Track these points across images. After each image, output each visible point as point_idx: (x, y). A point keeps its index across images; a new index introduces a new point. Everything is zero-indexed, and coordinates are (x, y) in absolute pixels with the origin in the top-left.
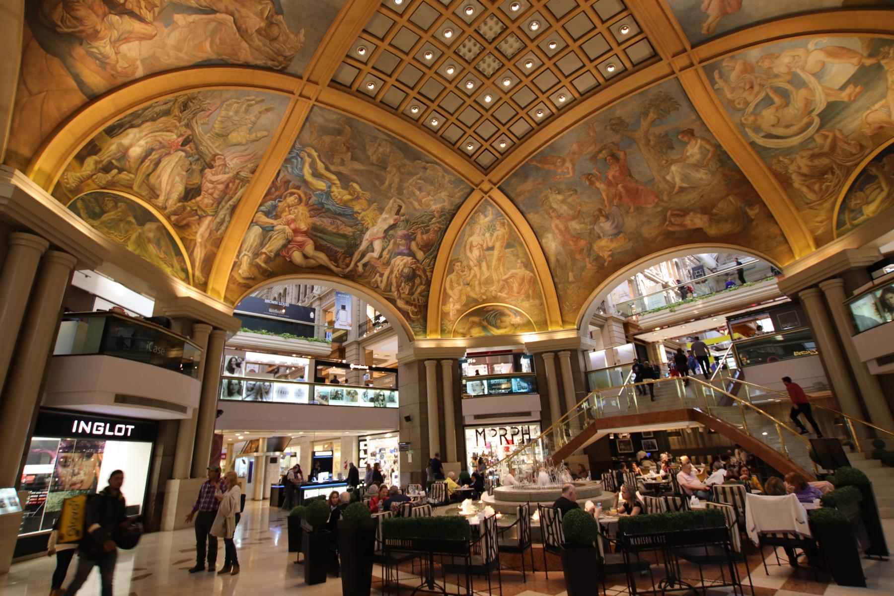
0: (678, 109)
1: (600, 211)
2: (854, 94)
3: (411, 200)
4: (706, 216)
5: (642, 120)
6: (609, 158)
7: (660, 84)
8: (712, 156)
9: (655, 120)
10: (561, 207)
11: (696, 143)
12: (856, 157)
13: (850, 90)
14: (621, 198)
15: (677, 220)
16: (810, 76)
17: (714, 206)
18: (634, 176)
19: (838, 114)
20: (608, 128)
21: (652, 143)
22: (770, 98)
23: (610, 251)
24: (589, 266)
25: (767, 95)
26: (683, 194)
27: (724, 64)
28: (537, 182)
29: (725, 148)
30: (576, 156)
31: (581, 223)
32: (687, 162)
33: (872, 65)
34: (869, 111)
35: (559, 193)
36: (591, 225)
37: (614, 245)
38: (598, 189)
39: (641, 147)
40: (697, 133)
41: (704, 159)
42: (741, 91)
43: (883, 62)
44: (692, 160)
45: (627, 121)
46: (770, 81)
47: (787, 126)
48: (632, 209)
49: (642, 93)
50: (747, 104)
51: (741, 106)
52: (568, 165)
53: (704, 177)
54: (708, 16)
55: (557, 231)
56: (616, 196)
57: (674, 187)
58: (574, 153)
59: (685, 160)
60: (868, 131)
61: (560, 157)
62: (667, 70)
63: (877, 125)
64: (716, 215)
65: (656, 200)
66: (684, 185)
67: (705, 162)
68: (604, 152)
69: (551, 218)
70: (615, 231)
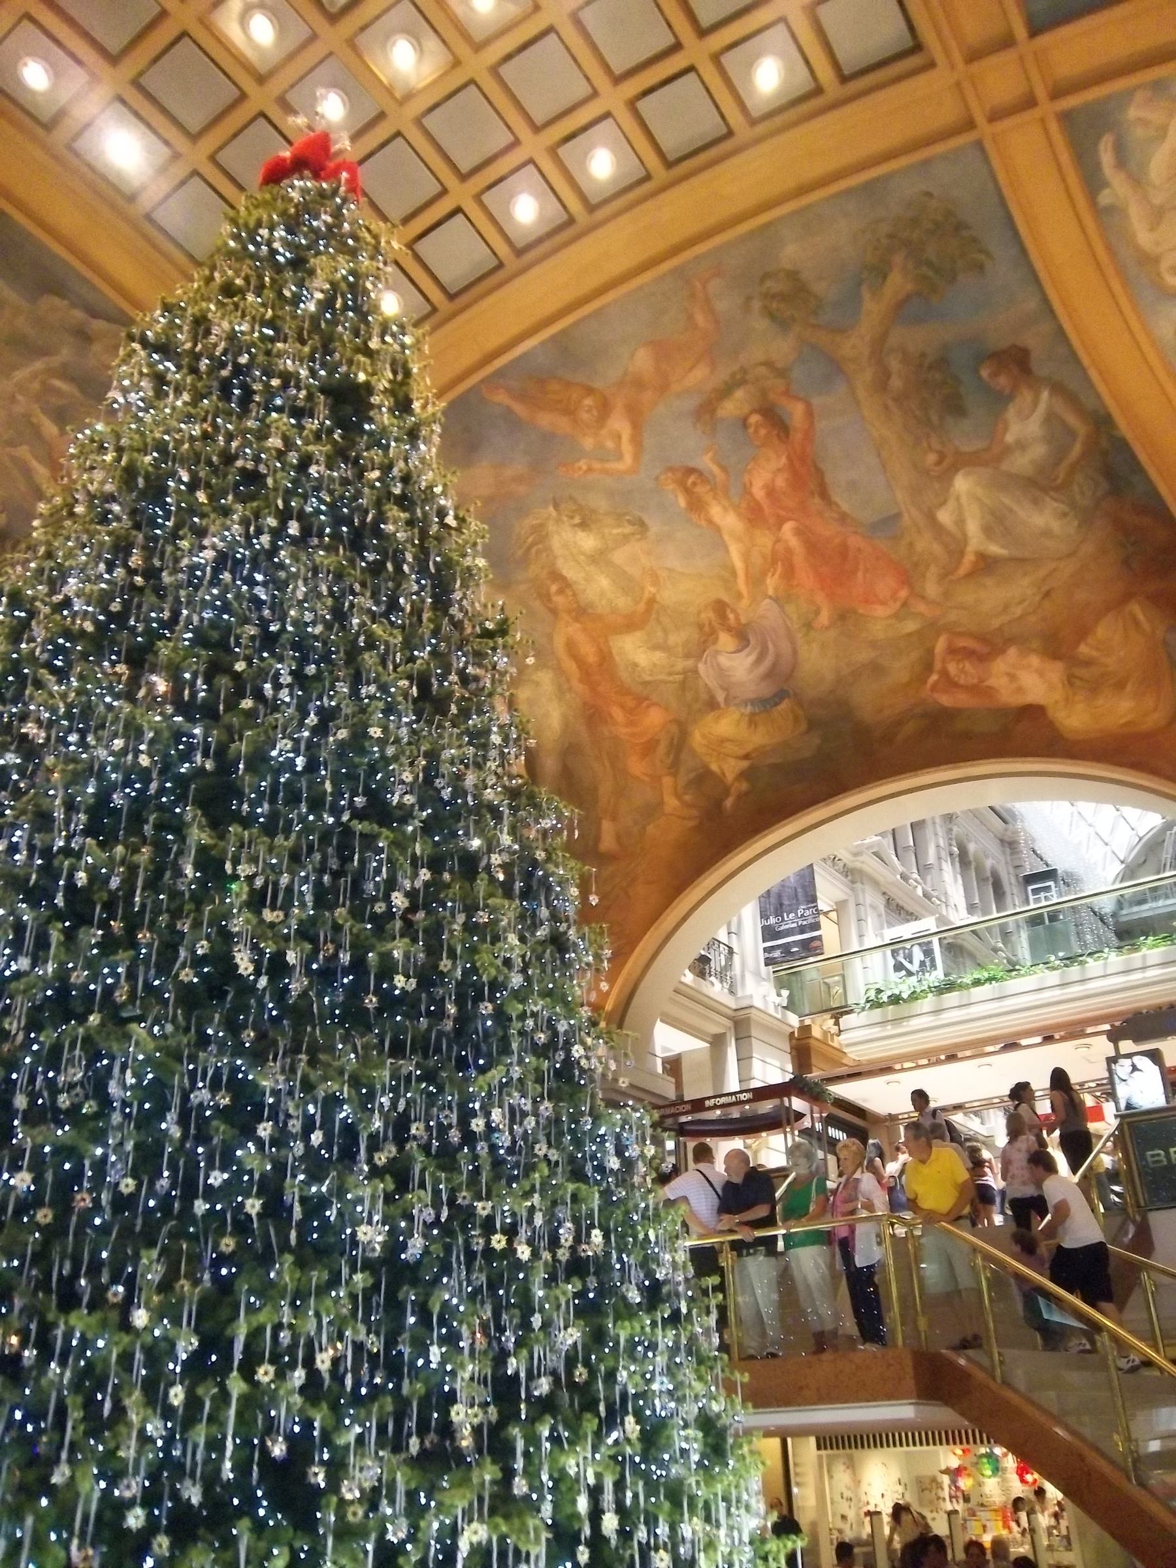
0: (981, 267)
1: (720, 608)
3: (23, 452)
4: (1059, 666)
5: (866, 295)
6: (755, 419)
7: (926, 162)
8: (1084, 455)
9: (908, 297)
10: (588, 579)
11: (1035, 404)
14: (790, 572)
15: (964, 671)
17: (1083, 633)
18: (836, 498)
20: (757, 305)
21: (896, 383)
23: (746, 757)
24: (671, 803)
26: (989, 581)
27: (1133, 113)
28: (509, 473)
29: (1124, 428)
30: (647, 396)
31: (656, 647)
32: (1005, 466)
35: (584, 525)
36: (687, 656)
37: (759, 738)
38: (718, 529)
39: (861, 393)
40: (1041, 368)
41: (1058, 462)
44: (1022, 463)
45: (819, 288)
48: (824, 617)
49: (868, 186)
52: (619, 424)
53: (1056, 526)
55: (570, 666)
56: (774, 562)
57: (962, 553)
58: (639, 384)
59: (999, 459)
61: (590, 391)
62: (947, 113)
64: (1088, 663)
65: (903, 593)
66: (995, 549)
67: (1062, 472)
68: (739, 394)
69: (554, 612)
70: (766, 690)
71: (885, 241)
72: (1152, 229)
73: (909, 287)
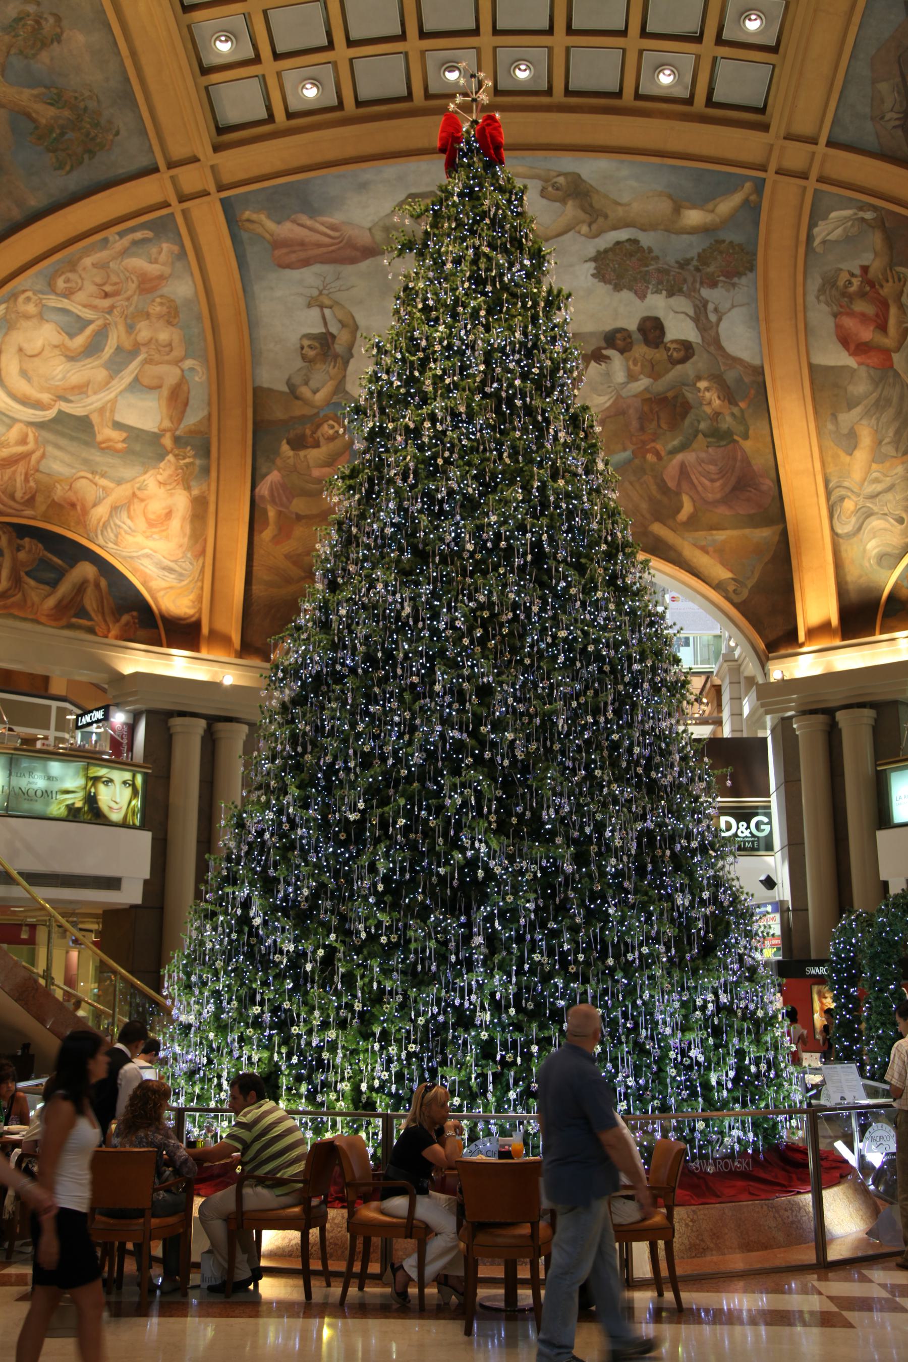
0: (60, 166)
2: (111, 444)
9: (34, 121)
12: (12, 503)
13: (117, 435)
16: (133, 375)
19: (72, 438)
22: (82, 329)
25: (90, 322)
27: (165, 246)
33: (164, 447)
34: (90, 476)
42: (98, 280)
43: (170, 457)
46: (120, 321)
47: (24, 373)
50: (68, 294)
51: (60, 284)
54: (279, 223)
60: (59, 493)
63: (74, 499)
71: (82, 105)
72: (93, 265)
73: (43, 121)
